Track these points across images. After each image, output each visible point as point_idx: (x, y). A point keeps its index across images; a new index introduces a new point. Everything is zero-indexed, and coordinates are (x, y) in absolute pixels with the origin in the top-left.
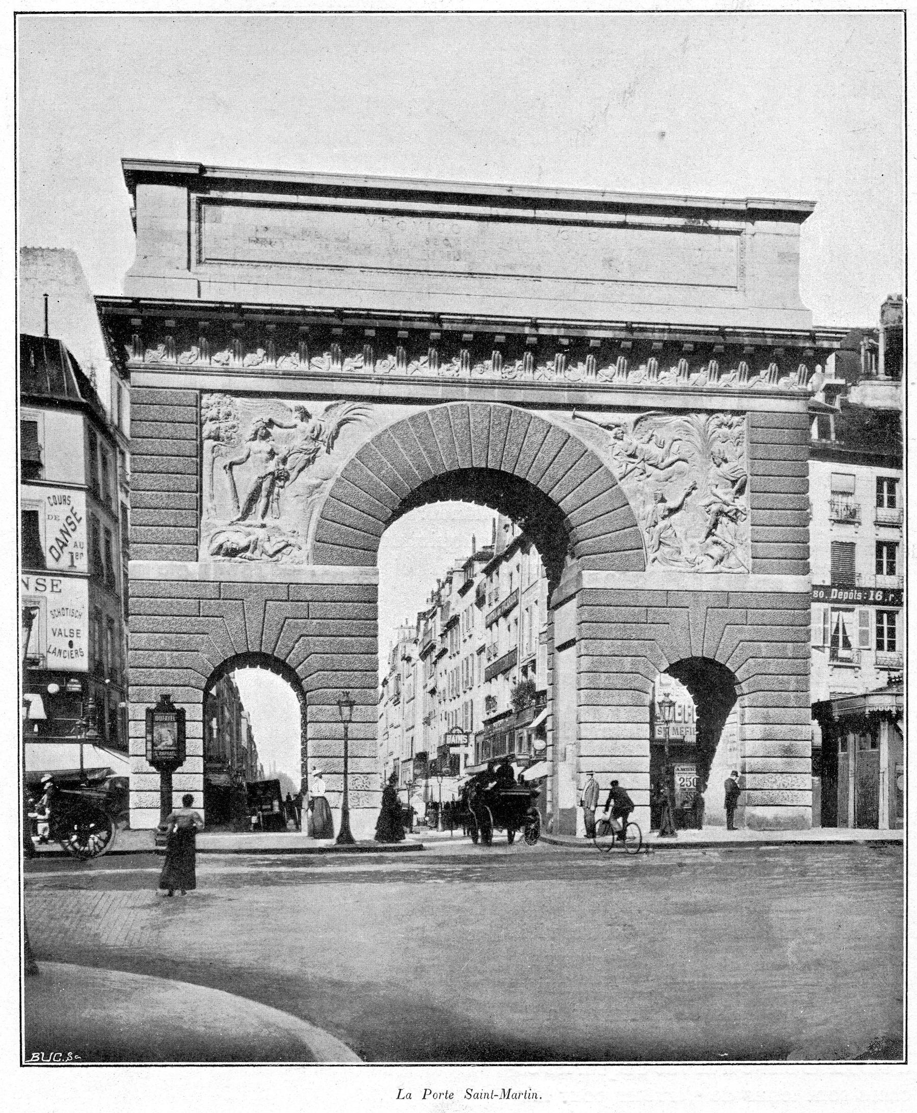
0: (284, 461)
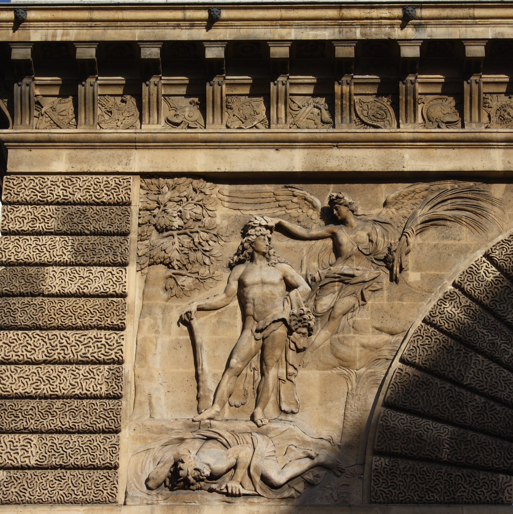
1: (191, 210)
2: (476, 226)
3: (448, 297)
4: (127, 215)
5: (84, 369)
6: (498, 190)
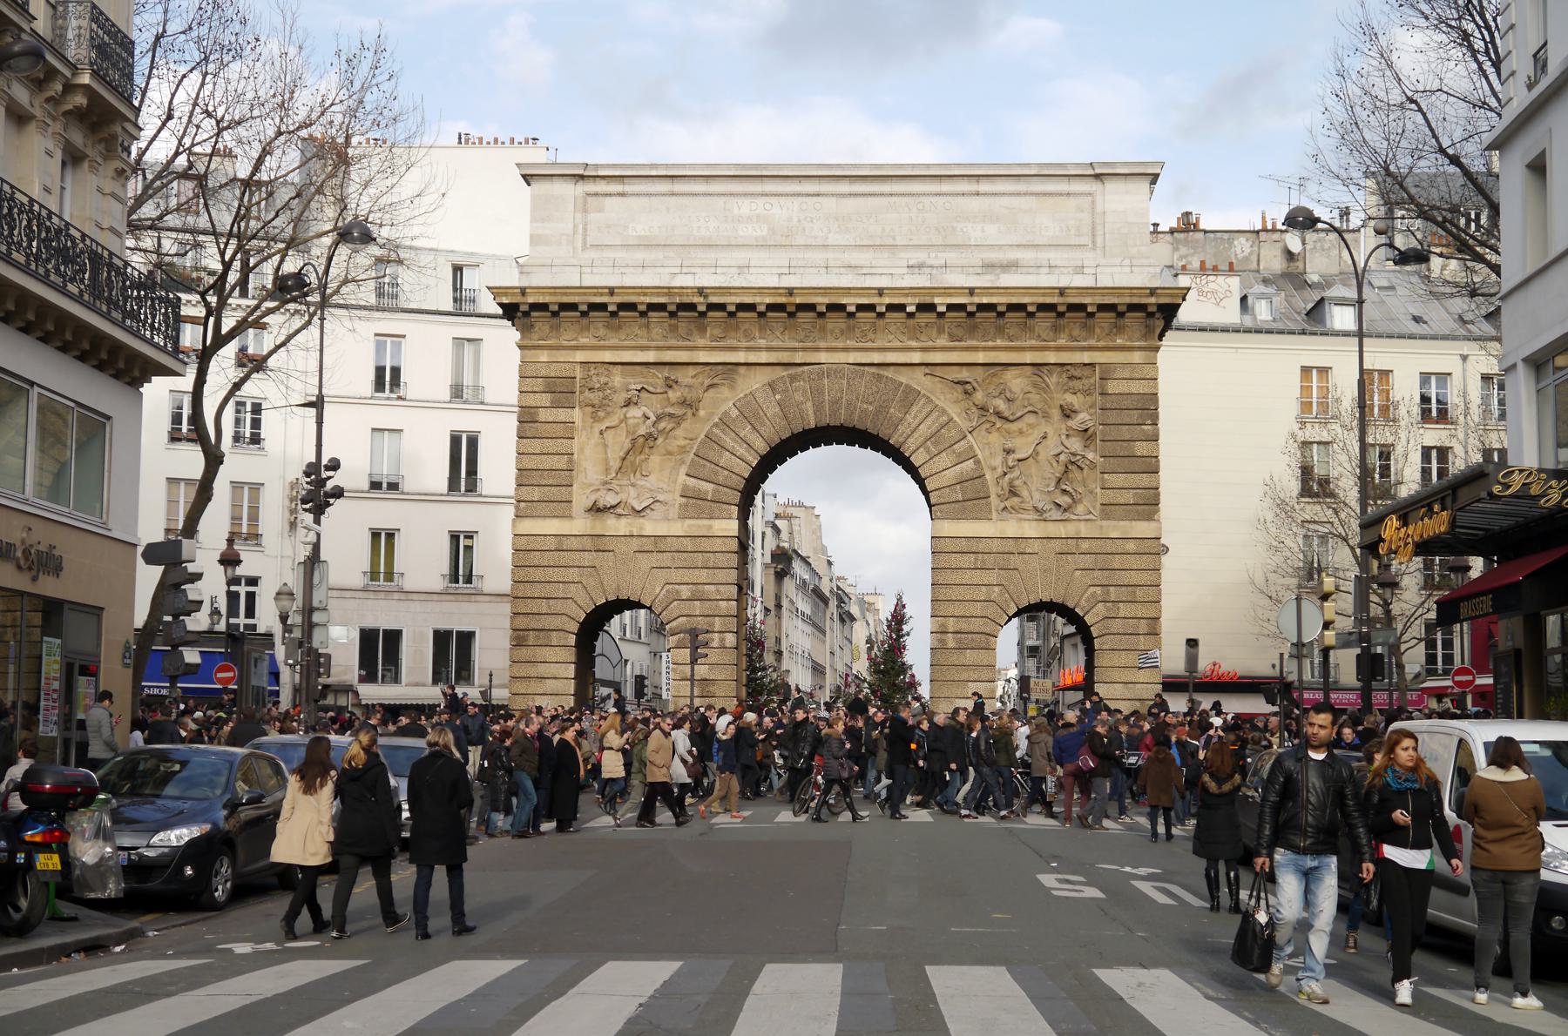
1: (603, 379)
2: (732, 388)
3: (716, 425)
4: (574, 384)
6: (742, 370)
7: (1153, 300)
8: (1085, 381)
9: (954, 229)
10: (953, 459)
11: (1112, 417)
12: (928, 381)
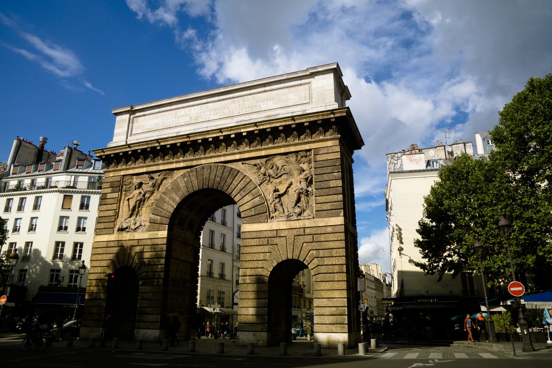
0: (144, 195)
1: (129, 181)
2: (172, 178)
3: (163, 193)
5: (110, 211)
7: (332, 116)
8: (308, 158)
9: (256, 106)
10: (251, 197)
11: (319, 171)
12: (243, 167)
